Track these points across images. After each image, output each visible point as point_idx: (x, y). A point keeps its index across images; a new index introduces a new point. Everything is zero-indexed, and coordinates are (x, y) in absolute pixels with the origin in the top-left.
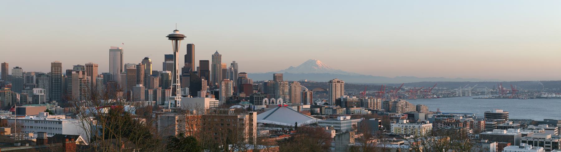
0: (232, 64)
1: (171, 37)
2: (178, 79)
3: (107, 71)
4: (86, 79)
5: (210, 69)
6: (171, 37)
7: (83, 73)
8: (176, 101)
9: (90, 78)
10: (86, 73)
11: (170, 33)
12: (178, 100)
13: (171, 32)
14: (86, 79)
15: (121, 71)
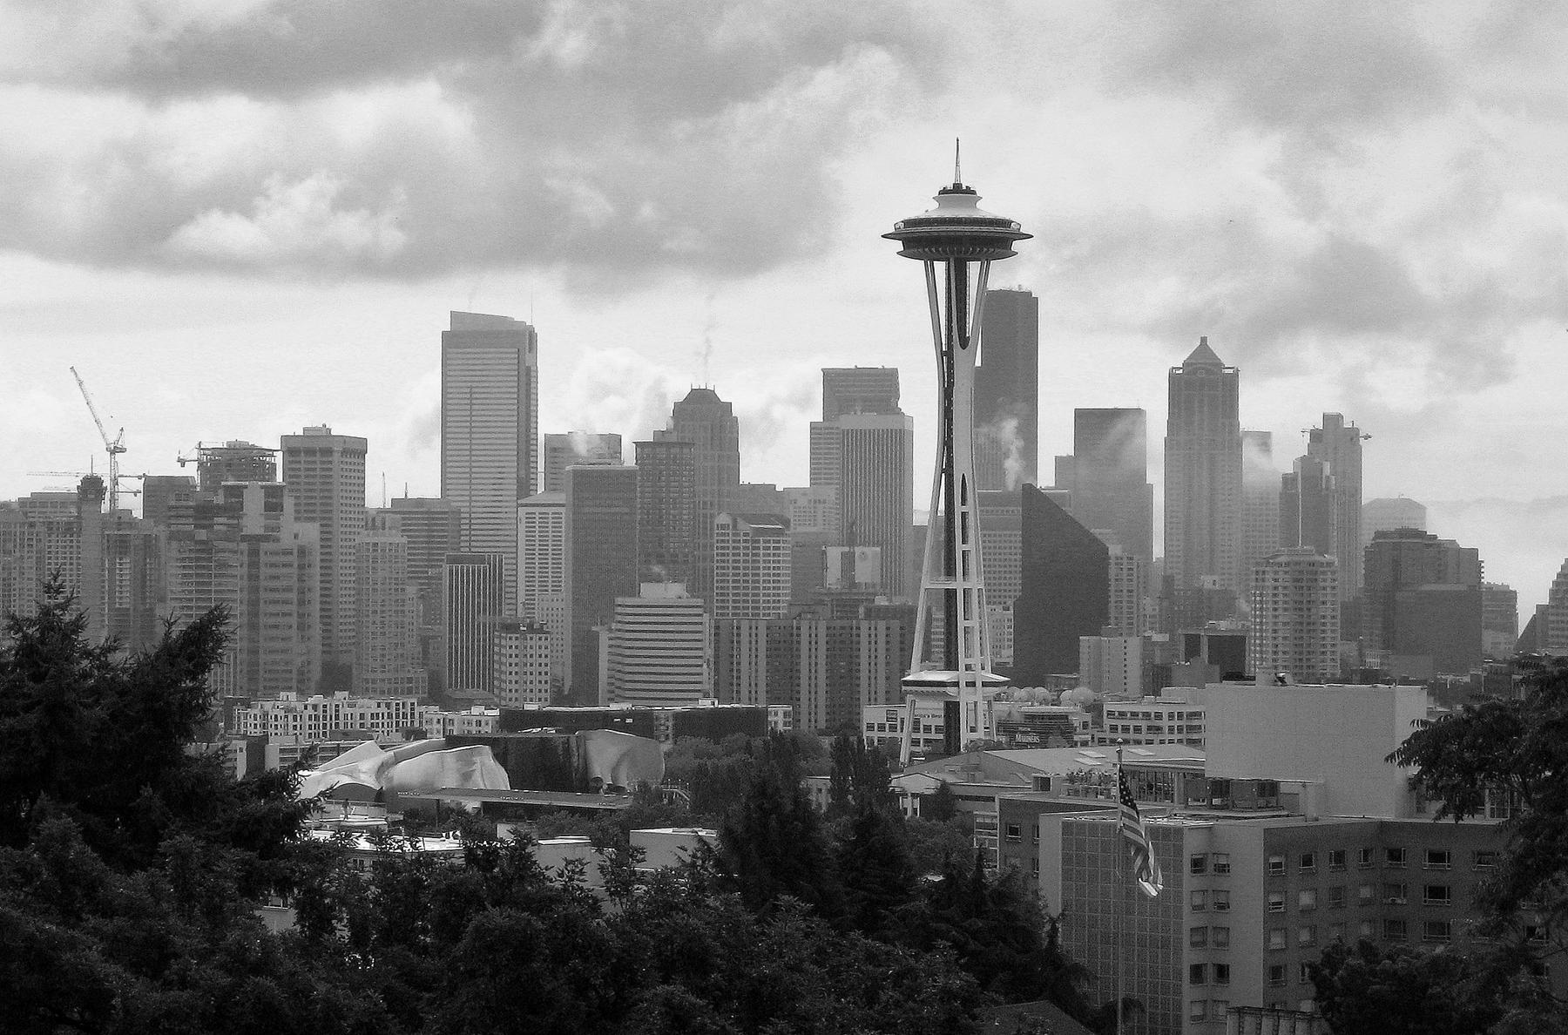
0: (1316, 436)
1: (920, 240)
2: (971, 547)
3: (425, 483)
4: (286, 540)
5: (1156, 476)
6: (920, 240)
7: (273, 503)
8: (952, 709)
9: (310, 532)
10: (289, 503)
11: (912, 215)
12: (965, 698)
13: (925, 206)
14: (286, 540)
15: (525, 487)
